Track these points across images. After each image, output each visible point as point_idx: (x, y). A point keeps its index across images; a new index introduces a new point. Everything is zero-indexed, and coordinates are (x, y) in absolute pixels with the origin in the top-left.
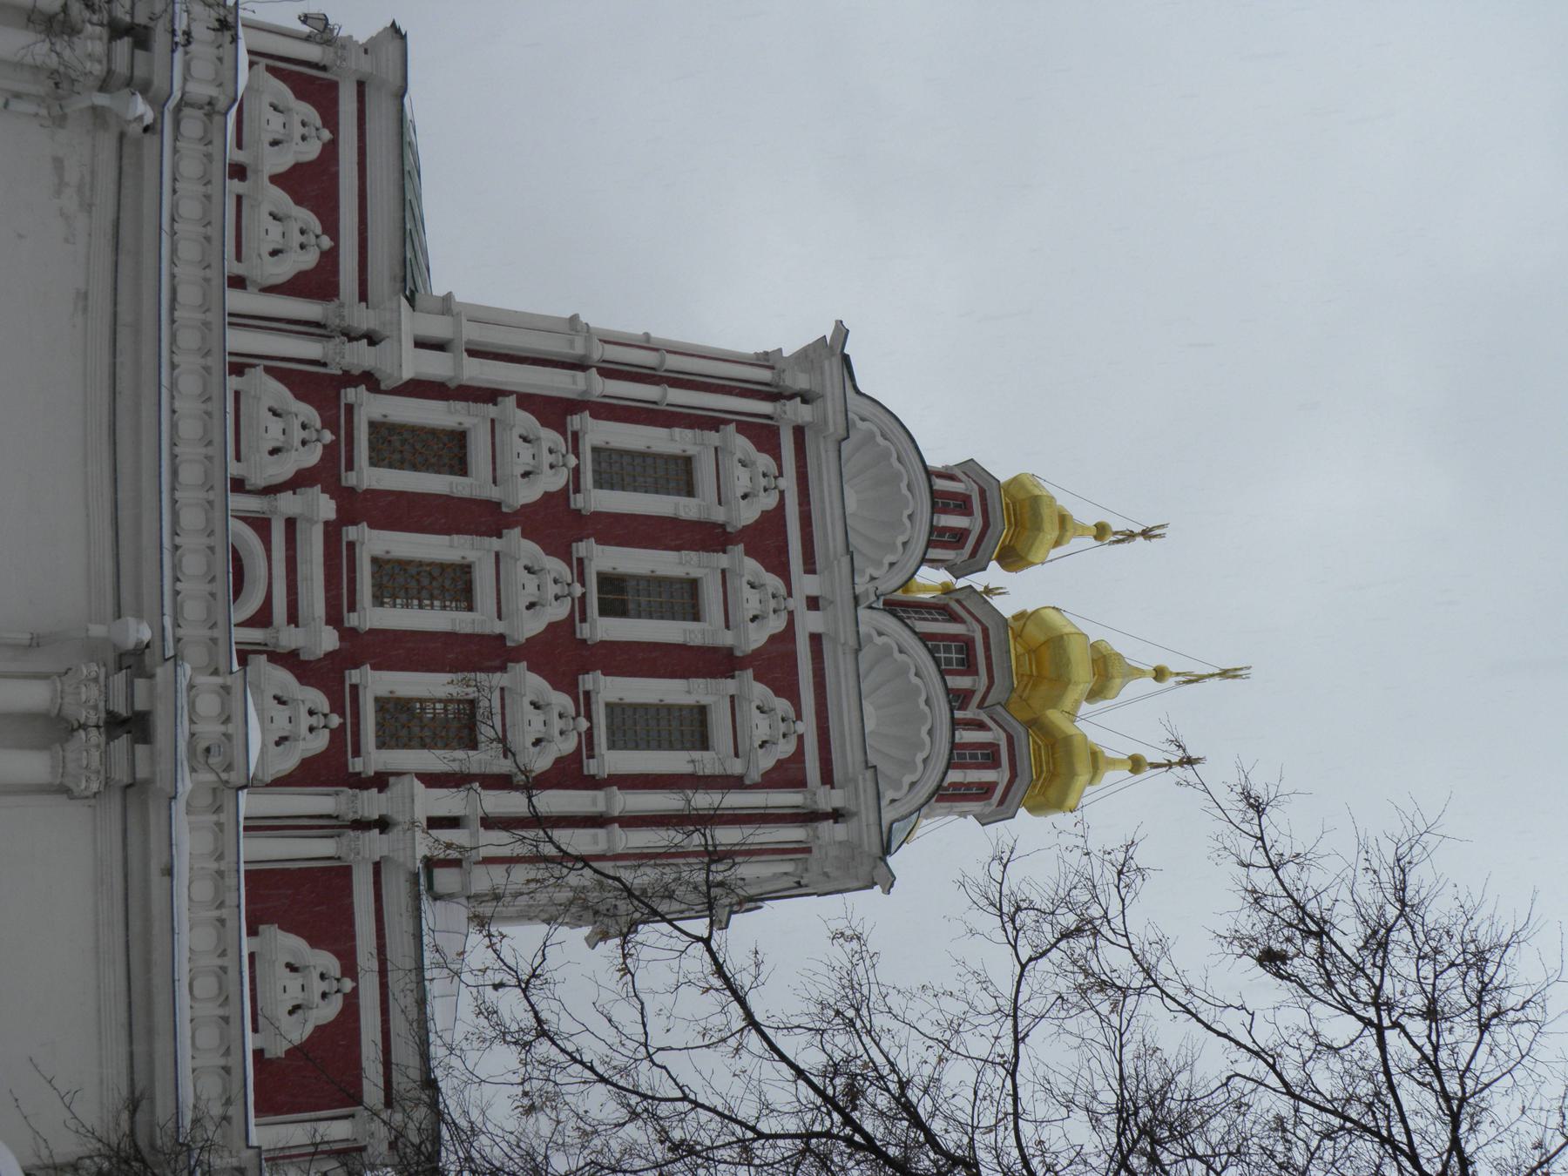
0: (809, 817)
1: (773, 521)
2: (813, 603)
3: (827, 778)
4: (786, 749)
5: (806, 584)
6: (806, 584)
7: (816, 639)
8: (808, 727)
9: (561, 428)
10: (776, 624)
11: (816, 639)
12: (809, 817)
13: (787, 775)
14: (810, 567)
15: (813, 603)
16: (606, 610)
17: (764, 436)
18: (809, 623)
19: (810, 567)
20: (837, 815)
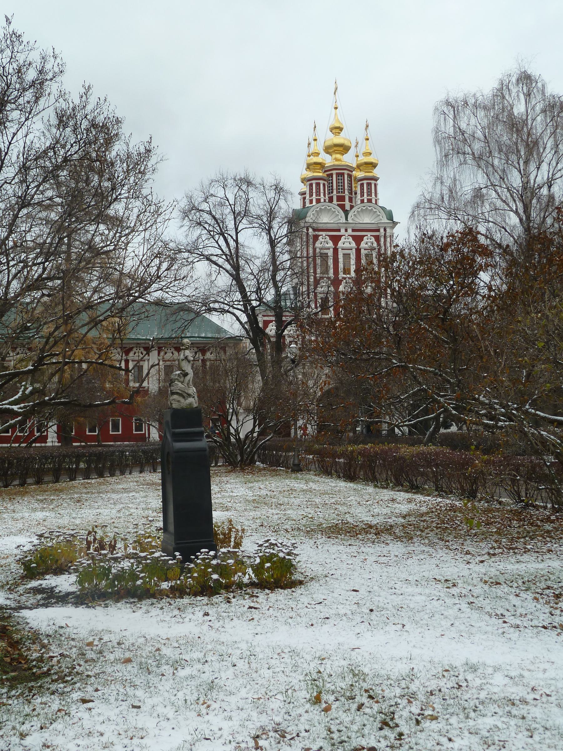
0: (385, 237)
1: (332, 238)
2: (346, 230)
3: (378, 230)
4: (373, 239)
5: (343, 231)
7: (353, 230)
8: (369, 234)
9: (319, 280)
10: (351, 239)
11: (353, 230)
12: (385, 237)
13: (377, 238)
15: (346, 230)
16: (349, 274)
17: (316, 238)
18: (350, 231)
19: (339, 230)
20: (385, 230)
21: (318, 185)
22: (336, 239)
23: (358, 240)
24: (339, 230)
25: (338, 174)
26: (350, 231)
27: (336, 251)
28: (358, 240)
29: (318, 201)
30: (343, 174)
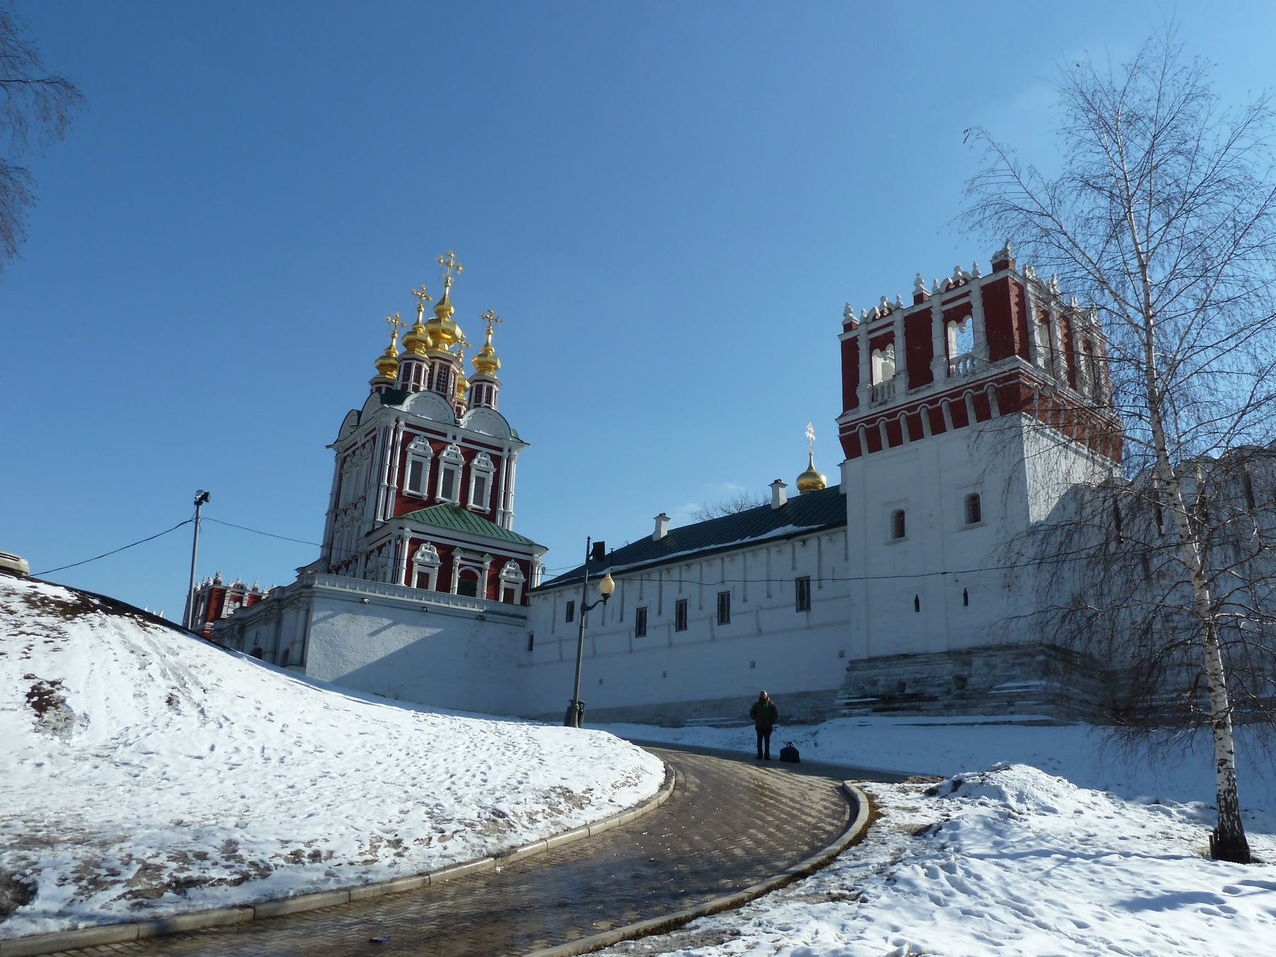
1: (432, 441)
2: (454, 438)
5: (449, 439)
6: (449, 439)
8: (485, 450)
11: (464, 440)
14: (445, 435)
15: (454, 438)
18: (459, 438)
21: (419, 368)
22: (439, 446)
23: (470, 455)
24: (445, 435)
25: (441, 366)
26: (459, 438)
27: (435, 463)
28: (470, 455)
29: (416, 389)
30: (449, 367)
